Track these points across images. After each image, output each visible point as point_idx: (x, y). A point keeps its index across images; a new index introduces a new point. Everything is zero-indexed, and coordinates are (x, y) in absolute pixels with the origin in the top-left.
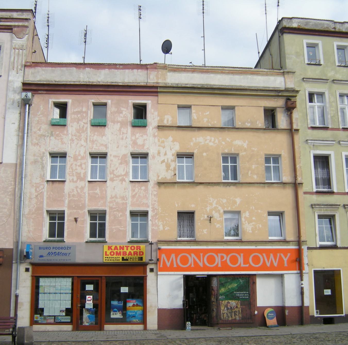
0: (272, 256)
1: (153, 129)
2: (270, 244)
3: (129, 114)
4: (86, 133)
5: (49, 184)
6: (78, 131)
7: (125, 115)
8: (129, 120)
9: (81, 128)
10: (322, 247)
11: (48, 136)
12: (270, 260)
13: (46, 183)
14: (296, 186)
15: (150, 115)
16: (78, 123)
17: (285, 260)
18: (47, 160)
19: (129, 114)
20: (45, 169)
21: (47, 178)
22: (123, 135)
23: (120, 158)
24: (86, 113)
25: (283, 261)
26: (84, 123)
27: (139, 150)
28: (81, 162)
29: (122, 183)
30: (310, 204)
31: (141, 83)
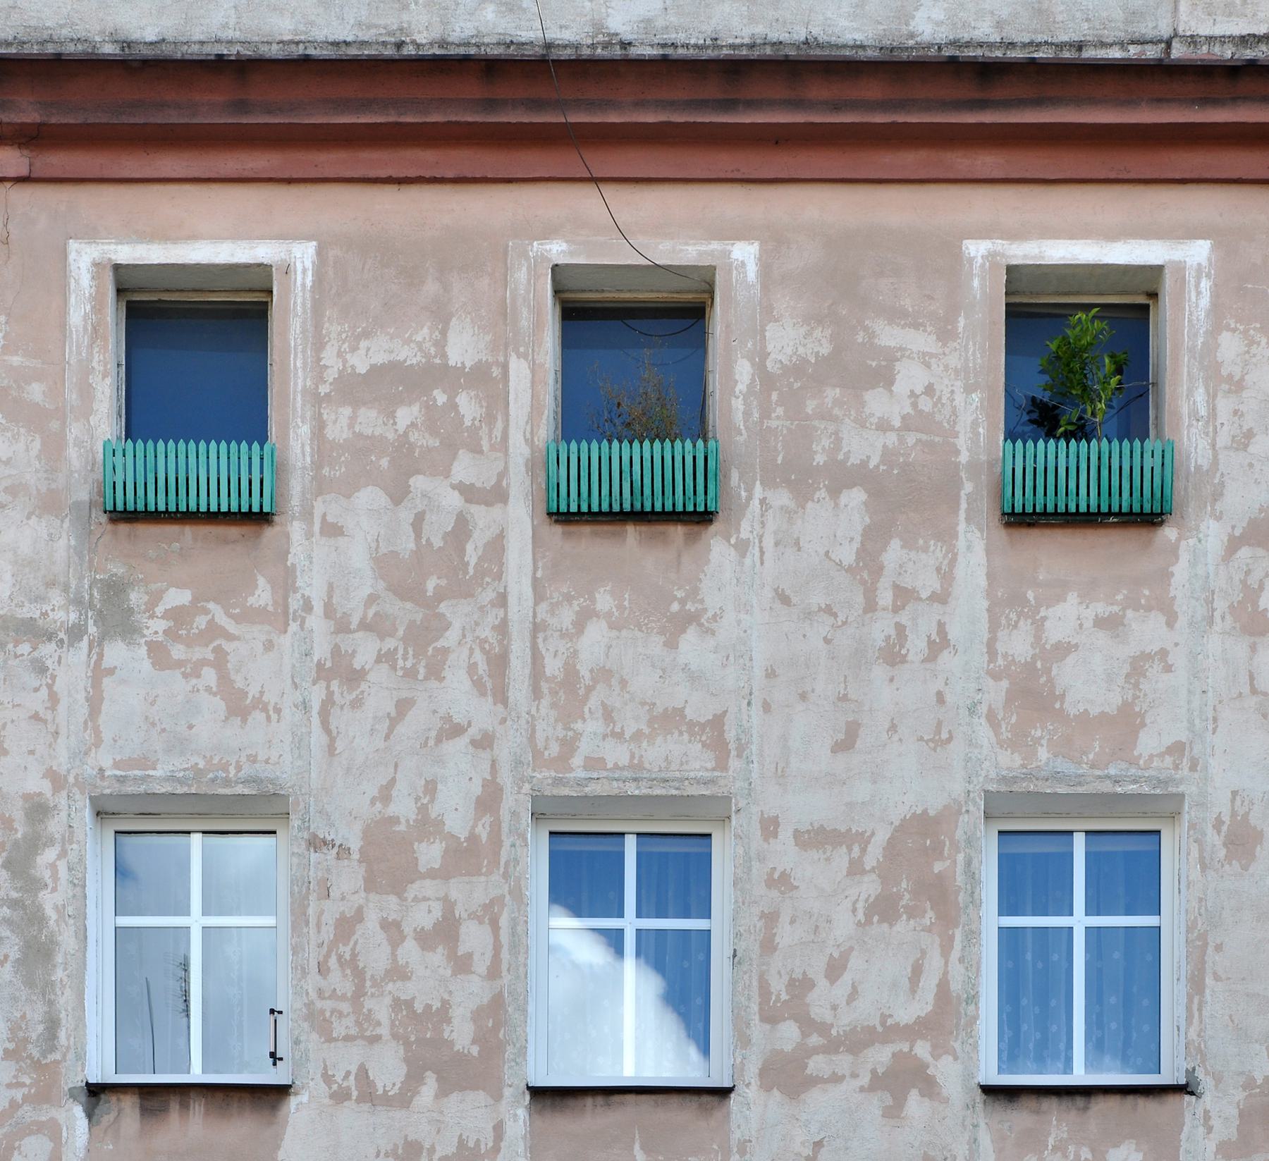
1: (1233, 545)
3: (968, 390)
4: (488, 595)
5: (107, 1119)
6: (400, 577)
7: (926, 404)
8: (964, 458)
9: (438, 543)
11: (76, 633)
13: (78, 1111)
15: (1200, 396)
16: (399, 494)
18: (79, 884)
19: (968, 390)
20: (59, 974)
21: (81, 1057)
22: (904, 618)
23: (874, 855)
24: (487, 380)
26: (468, 492)
27: (1084, 769)
28: (449, 905)
29: (894, 1112)
31: (1103, 45)
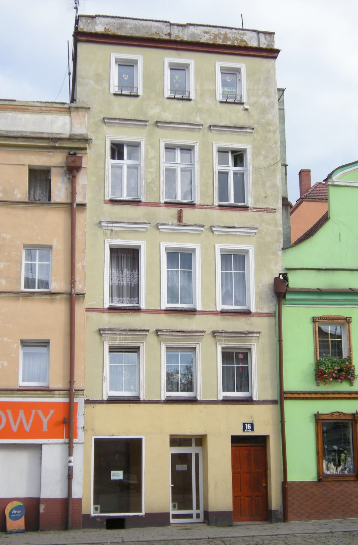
0: (22, 414)
2: (19, 394)
10: (113, 401)
12: (19, 420)
14: (72, 297)
17: (45, 421)
25: (42, 423)
30: (98, 329)
